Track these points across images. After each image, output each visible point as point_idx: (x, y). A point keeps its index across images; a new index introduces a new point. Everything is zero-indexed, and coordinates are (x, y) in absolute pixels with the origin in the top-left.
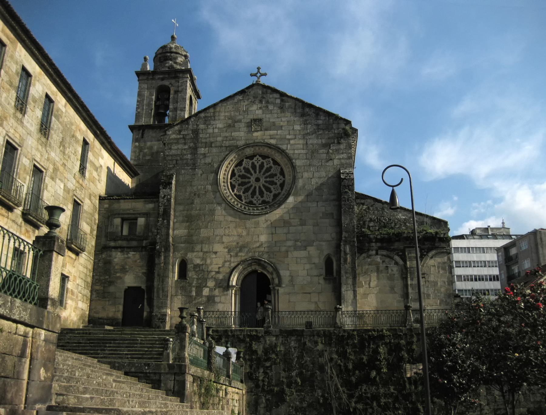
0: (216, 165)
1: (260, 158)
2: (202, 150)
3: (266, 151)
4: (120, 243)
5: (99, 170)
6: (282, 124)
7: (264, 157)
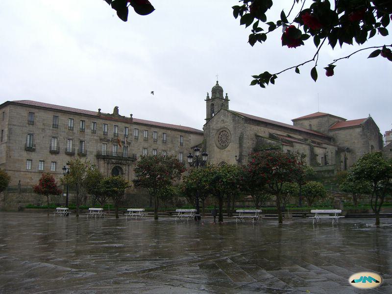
3: (225, 130)
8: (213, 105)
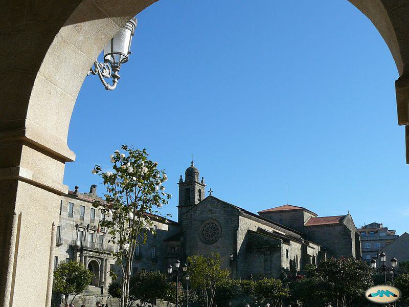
2: (193, 222)
7: (213, 223)
8: (188, 190)
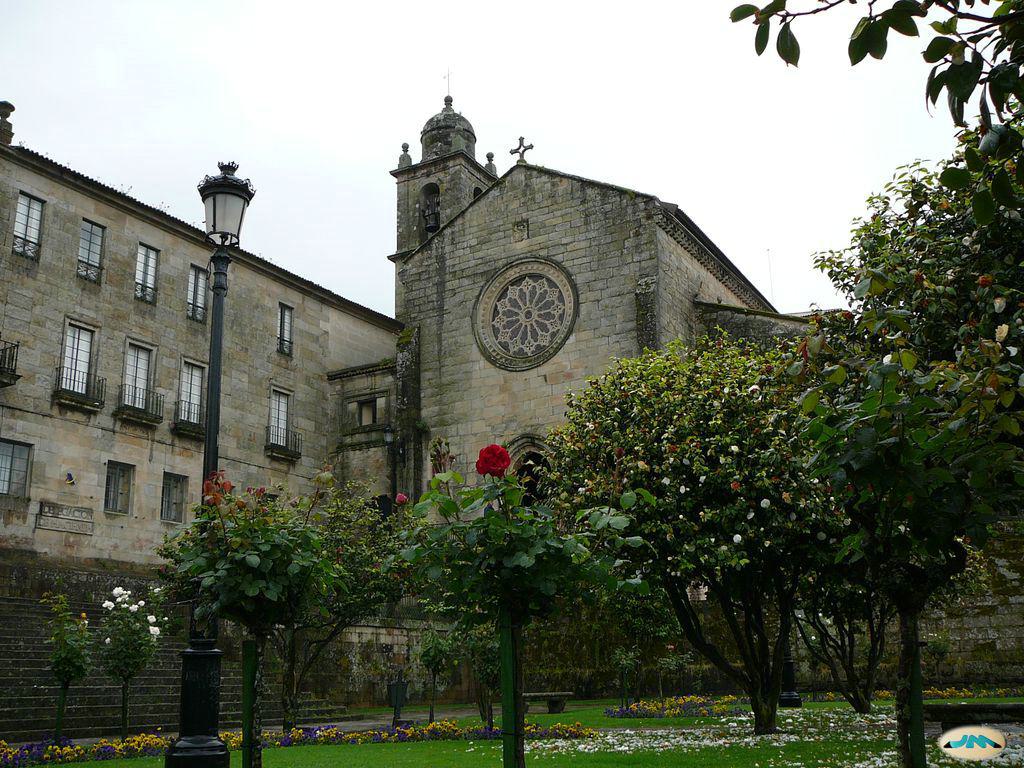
0: (470, 305)
1: (531, 282)
2: (449, 285)
3: (536, 268)
4: (358, 438)
5: (321, 339)
6: (554, 221)
8: (432, 190)
